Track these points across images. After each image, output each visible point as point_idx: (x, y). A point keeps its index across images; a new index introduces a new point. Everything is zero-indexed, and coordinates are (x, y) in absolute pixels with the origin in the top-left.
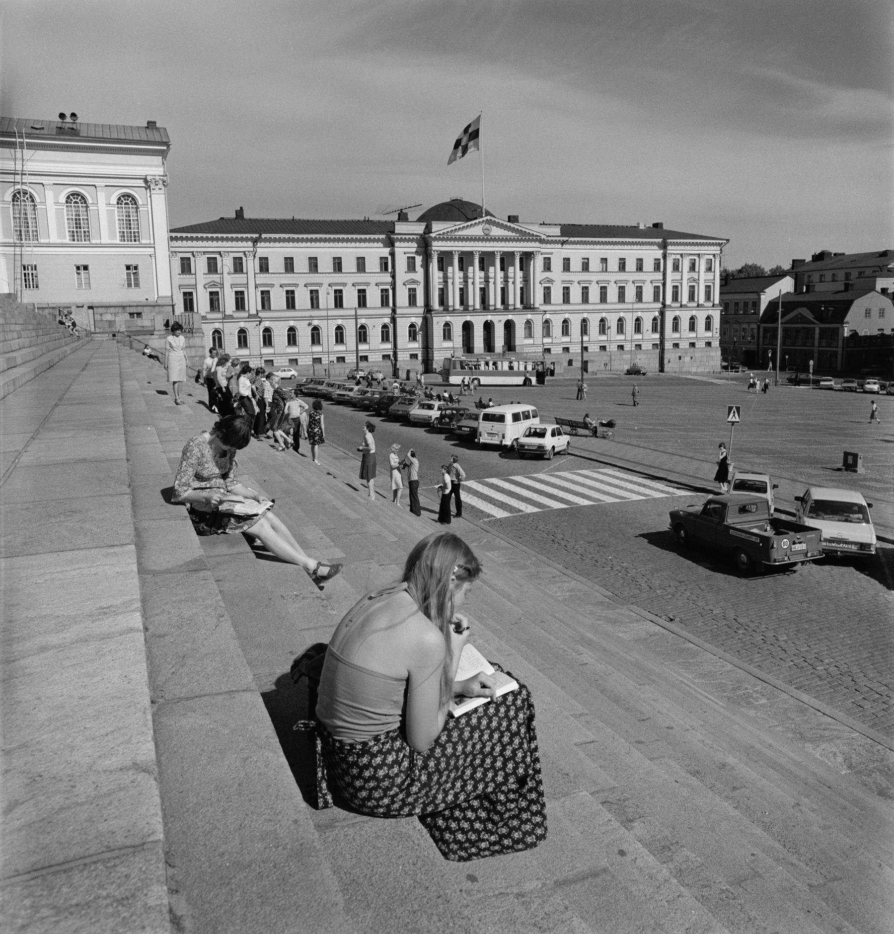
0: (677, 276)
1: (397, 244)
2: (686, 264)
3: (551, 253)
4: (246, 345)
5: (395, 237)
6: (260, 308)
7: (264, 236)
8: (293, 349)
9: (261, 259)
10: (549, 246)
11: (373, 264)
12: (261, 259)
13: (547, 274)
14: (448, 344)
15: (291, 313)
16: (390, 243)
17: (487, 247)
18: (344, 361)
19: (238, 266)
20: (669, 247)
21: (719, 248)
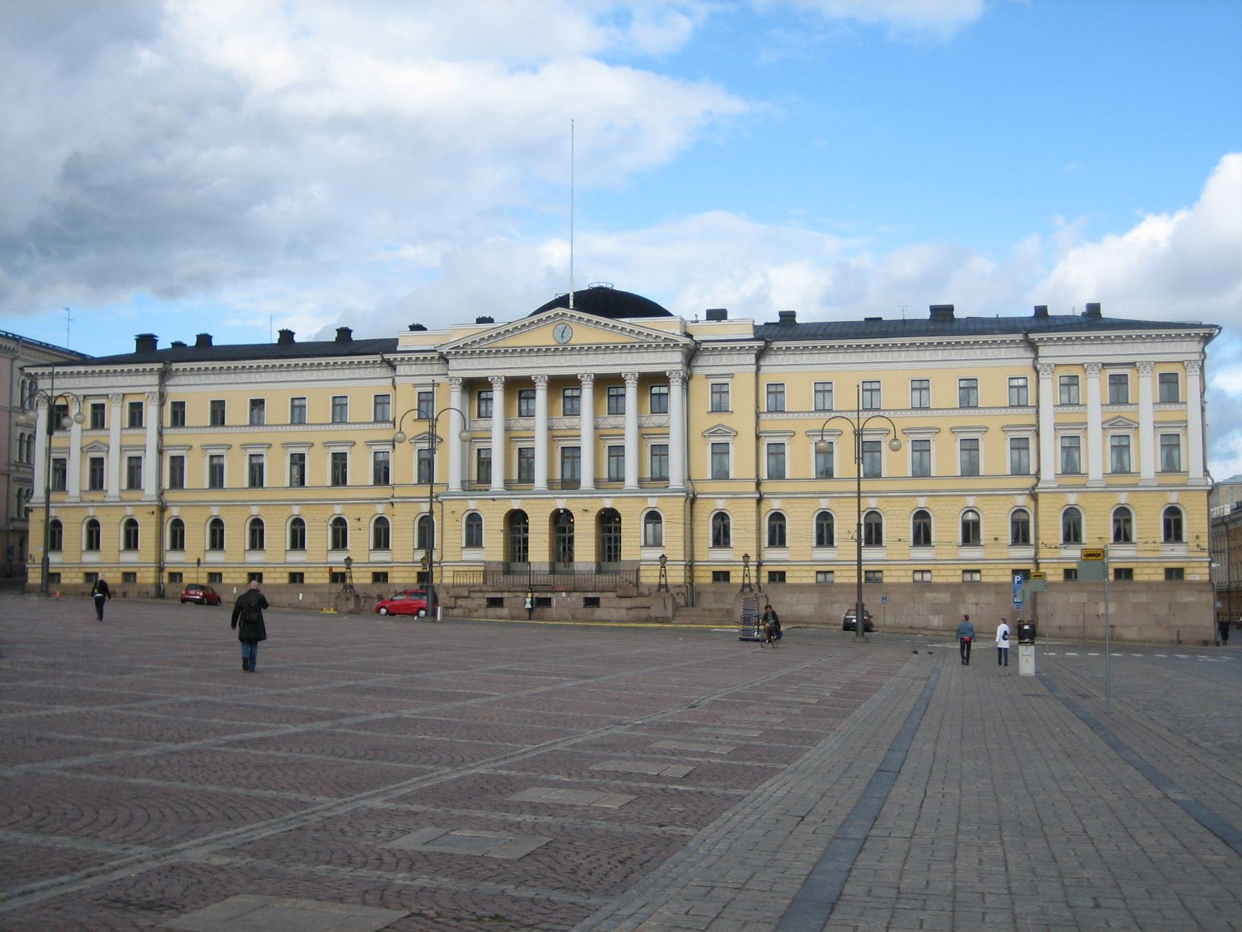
0: (1070, 415)
1: (401, 370)
2: (1095, 389)
3: (731, 376)
4: (386, 546)
5: (399, 356)
6: (166, 483)
7: (175, 366)
8: (381, 556)
9: (174, 404)
10: (725, 359)
11: (359, 408)
12: (174, 404)
13: (722, 419)
14: (473, 554)
15: (216, 495)
16: (391, 365)
17: (563, 366)
18: (302, 580)
19: (136, 416)
20: (1043, 351)
21: (1195, 346)
